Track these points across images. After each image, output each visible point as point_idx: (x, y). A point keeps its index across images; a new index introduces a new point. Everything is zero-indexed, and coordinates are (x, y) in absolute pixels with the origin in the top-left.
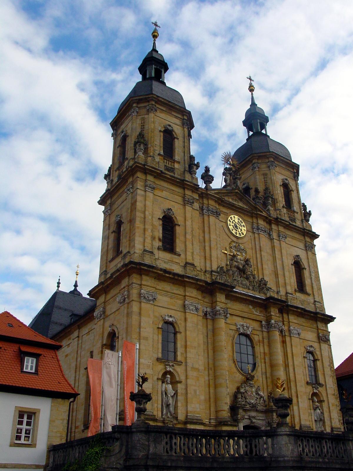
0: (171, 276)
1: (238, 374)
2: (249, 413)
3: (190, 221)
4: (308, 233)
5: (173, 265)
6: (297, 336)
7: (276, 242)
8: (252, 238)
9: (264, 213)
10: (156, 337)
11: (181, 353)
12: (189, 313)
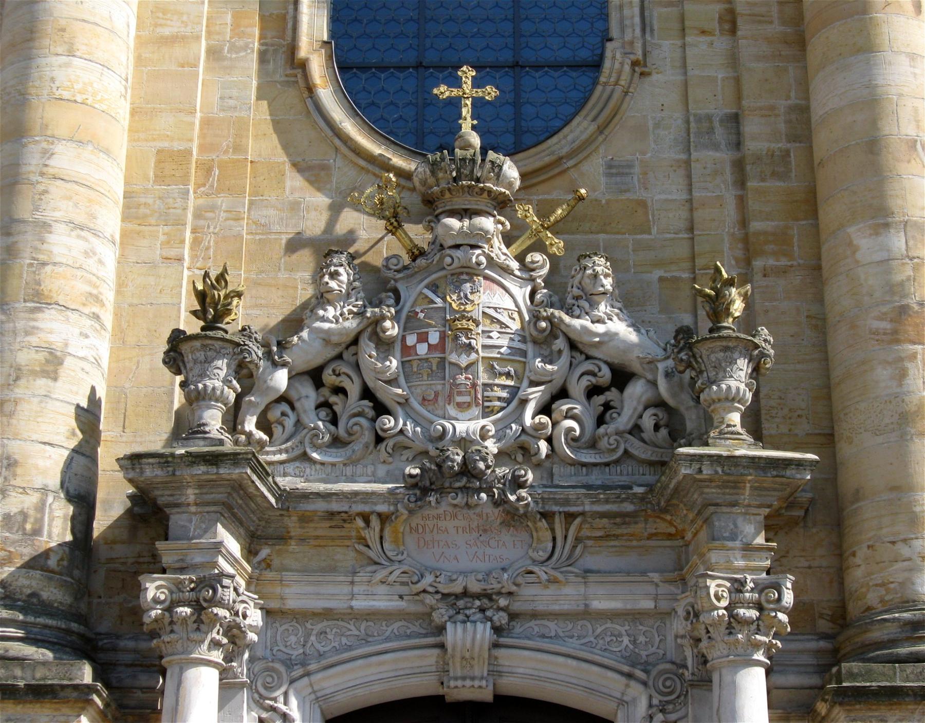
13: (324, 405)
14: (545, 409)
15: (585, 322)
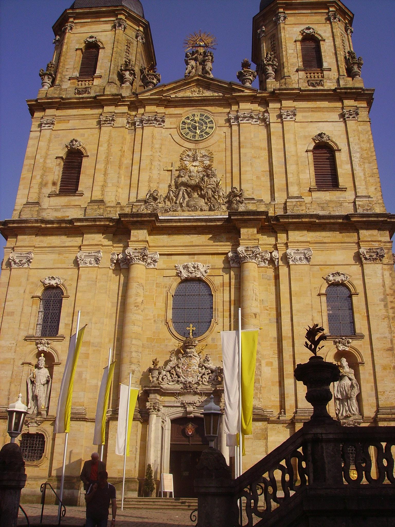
0: (55, 225)
1: (174, 340)
2: (181, 398)
3: (106, 145)
4: (346, 93)
5: (68, 210)
6: (305, 262)
7: (275, 128)
8: (228, 134)
9: (246, 91)
10: (27, 309)
11: (66, 325)
12: (84, 267)
13: (171, 376)
14: (202, 377)
15: (207, 365)
